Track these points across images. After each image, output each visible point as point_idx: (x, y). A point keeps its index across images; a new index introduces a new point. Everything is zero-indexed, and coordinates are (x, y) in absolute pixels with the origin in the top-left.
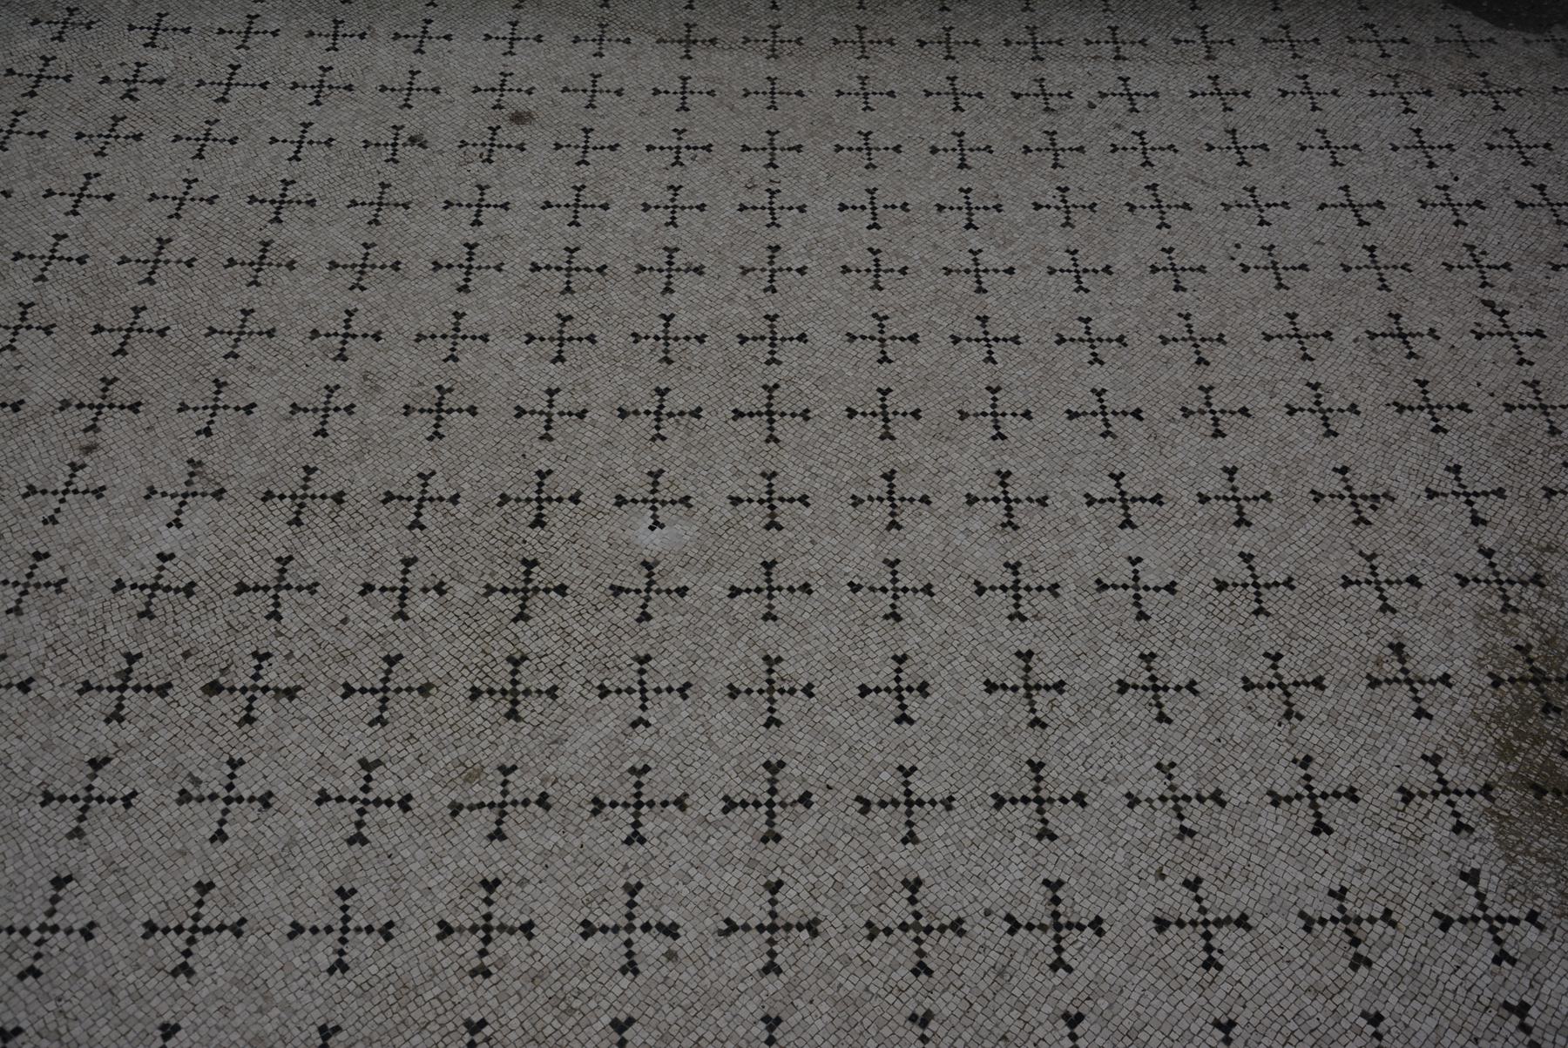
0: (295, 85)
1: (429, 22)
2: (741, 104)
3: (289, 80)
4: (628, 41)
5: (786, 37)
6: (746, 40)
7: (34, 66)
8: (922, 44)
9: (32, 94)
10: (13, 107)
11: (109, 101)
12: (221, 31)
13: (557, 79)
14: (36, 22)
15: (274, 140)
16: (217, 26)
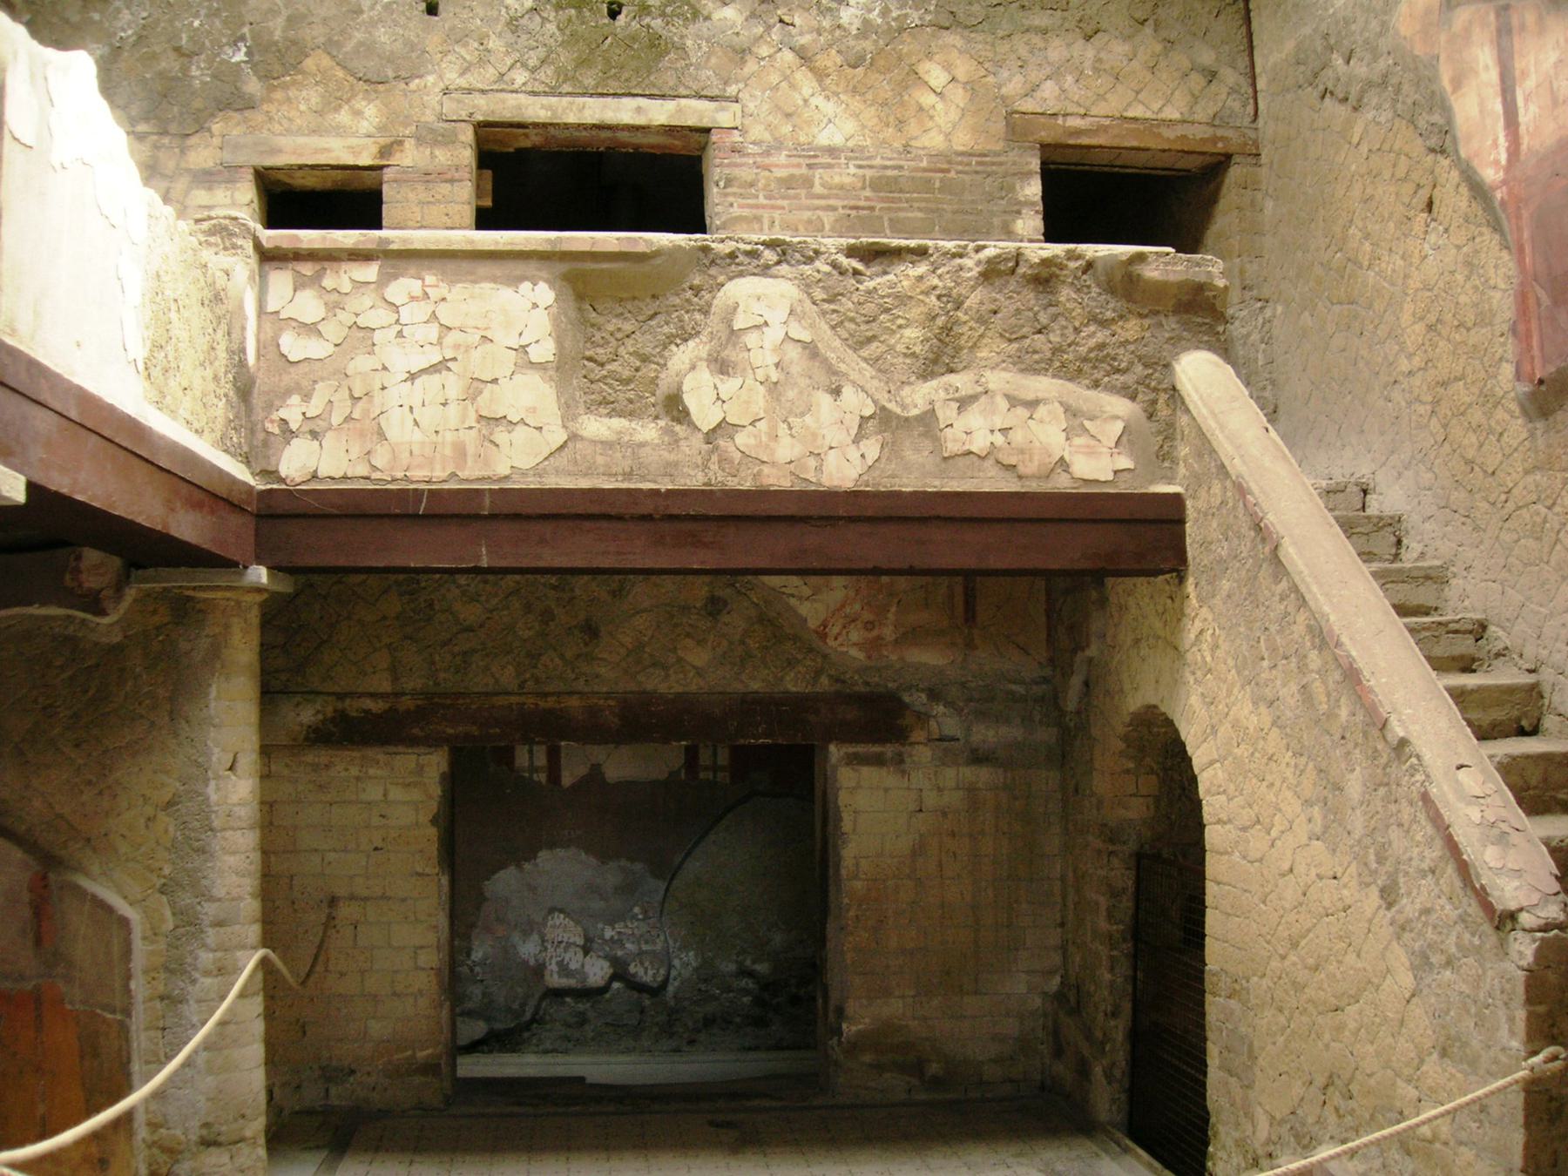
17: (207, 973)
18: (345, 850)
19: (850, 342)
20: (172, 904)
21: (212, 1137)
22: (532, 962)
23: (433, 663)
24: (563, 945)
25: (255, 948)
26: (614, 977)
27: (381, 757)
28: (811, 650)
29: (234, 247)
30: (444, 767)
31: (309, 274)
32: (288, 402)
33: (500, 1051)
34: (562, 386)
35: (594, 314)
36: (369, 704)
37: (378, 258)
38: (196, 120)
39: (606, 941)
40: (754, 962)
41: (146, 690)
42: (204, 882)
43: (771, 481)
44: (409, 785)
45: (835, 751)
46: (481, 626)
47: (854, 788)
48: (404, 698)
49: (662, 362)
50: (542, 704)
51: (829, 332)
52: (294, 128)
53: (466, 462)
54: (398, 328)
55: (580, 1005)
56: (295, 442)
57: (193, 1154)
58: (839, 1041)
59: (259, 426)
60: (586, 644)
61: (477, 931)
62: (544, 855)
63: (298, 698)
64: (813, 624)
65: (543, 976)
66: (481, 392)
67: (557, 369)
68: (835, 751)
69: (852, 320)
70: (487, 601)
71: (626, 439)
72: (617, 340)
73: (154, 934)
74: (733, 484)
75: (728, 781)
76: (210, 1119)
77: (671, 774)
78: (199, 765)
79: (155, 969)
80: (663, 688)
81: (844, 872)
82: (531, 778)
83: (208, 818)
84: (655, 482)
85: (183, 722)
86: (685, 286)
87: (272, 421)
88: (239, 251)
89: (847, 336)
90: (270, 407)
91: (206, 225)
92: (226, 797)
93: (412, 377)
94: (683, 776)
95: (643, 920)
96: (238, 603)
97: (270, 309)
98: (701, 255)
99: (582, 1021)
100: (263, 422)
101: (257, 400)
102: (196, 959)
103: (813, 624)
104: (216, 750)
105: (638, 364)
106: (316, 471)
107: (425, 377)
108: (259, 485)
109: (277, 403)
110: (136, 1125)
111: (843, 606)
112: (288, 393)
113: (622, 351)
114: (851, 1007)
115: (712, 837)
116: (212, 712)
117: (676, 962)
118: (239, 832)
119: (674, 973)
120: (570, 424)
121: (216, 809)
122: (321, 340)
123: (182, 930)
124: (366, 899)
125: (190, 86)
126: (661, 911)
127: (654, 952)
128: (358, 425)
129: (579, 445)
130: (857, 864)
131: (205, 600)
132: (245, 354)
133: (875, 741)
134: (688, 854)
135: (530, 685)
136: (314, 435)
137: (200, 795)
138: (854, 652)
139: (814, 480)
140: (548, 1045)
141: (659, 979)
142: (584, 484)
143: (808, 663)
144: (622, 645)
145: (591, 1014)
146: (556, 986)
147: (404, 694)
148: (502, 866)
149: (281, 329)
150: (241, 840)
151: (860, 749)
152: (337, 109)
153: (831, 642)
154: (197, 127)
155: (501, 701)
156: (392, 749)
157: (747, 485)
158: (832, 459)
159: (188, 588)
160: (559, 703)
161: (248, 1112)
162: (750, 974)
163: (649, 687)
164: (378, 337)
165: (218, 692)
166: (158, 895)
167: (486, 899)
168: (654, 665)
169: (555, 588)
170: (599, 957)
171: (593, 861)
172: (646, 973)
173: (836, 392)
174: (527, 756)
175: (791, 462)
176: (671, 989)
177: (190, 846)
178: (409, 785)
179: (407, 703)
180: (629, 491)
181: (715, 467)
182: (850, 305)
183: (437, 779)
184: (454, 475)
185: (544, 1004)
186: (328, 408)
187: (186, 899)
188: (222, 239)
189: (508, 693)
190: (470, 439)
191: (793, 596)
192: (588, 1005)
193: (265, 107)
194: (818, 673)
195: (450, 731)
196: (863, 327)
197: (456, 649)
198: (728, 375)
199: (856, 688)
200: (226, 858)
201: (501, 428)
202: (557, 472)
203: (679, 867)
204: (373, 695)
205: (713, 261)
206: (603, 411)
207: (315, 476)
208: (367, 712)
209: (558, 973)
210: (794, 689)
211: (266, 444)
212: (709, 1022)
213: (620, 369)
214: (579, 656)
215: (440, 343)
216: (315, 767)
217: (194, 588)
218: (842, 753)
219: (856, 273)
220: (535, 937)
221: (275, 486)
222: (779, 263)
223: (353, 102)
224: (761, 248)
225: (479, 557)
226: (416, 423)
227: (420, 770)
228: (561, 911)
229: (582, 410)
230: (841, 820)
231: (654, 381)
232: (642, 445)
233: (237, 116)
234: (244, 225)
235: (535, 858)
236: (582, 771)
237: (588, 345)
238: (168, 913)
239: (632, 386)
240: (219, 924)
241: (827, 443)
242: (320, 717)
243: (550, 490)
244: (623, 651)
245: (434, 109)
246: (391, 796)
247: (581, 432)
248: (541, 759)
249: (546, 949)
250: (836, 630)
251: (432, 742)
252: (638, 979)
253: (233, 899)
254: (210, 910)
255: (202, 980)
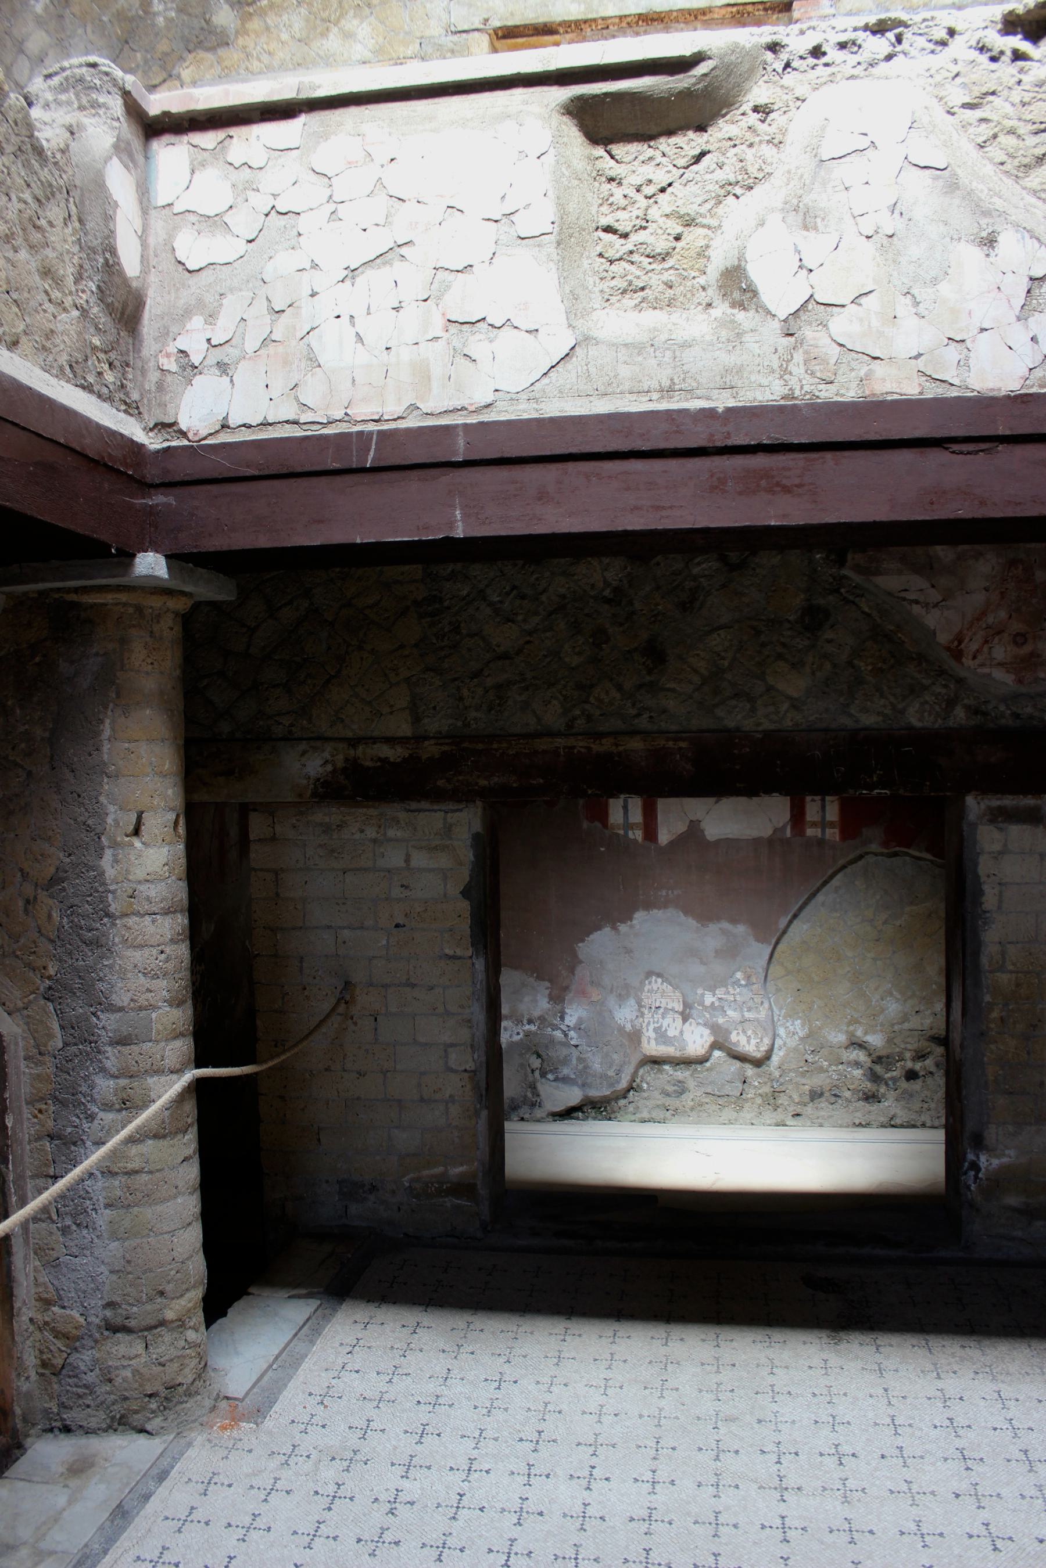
0: (503, 1510)
1: (593, 1467)
2: (830, 1539)
3: (499, 1506)
4: (737, 1487)
5: (853, 1488)
6: (824, 1489)
7: (331, 1489)
8: (957, 1496)
9: (330, 1509)
10: (317, 1518)
11: (378, 1516)
12: (452, 1469)
13: (689, 1514)
14: (333, 1459)
15: (490, 1551)
16: (449, 1465)
17: (107, 1107)
18: (362, 928)
19: (1008, 167)
20: (60, 1014)
21: (119, 1321)
22: (628, 1027)
23: (461, 699)
24: (662, 1010)
25: (179, 1071)
26: (715, 1046)
27: (402, 815)
28: (942, 672)
29: (95, 105)
30: (477, 826)
31: (210, 146)
32: (188, 327)
33: (595, 1119)
34: (566, 265)
35: (612, 163)
36: (386, 751)
37: (301, 111)
38: (163, 68)
39: (705, 1008)
40: (866, 1033)
41: (22, 729)
42: (100, 985)
43: (888, 387)
44: (436, 848)
45: (974, 805)
46: (519, 652)
47: (1000, 853)
48: (427, 743)
49: (713, 222)
50: (596, 748)
51: (975, 153)
52: (276, 63)
53: (430, 390)
54: (332, 207)
55: (679, 1073)
56: (198, 380)
57: (96, 1341)
58: (976, 1177)
59: (152, 364)
60: (650, 672)
61: (571, 995)
62: (639, 916)
63: (303, 746)
64: (943, 638)
65: (639, 1042)
66: (448, 287)
67: (559, 243)
68: (974, 805)
69: (1012, 132)
70: (525, 620)
71: (663, 337)
72: (646, 197)
73: (38, 1053)
74: (827, 394)
75: (838, 839)
76: (117, 1299)
77: (775, 830)
78: (89, 829)
79: (42, 1099)
80: (748, 725)
81: (984, 960)
82: (626, 833)
83: (103, 900)
84: (708, 398)
85: (66, 770)
86: (747, 107)
87: (168, 355)
88: (101, 112)
89: (1004, 158)
90: (165, 335)
91: (56, 80)
92: (128, 872)
93: (353, 272)
94: (788, 833)
95: (746, 985)
96: (139, 609)
97: (161, 202)
98: (769, 56)
99: (681, 1090)
100: (156, 356)
101: (148, 325)
102: (92, 1087)
103: (943, 638)
104: (112, 809)
105: (679, 229)
106: (226, 418)
107: (370, 273)
108: (153, 442)
109: (174, 329)
110: (17, 1305)
111: (984, 614)
112: (187, 313)
113: (654, 213)
114: (991, 1134)
115: (820, 897)
116: (106, 757)
117: (781, 1031)
118: (148, 918)
119: (778, 1042)
120: (579, 323)
121: (112, 888)
122: (229, 237)
123: (73, 1049)
124: (385, 986)
125: (154, 25)
126: (766, 977)
127: (757, 1020)
128: (281, 349)
129: (593, 351)
130: (1003, 954)
131: (93, 606)
132: (113, 251)
133: (1025, 792)
134: (795, 916)
135: (581, 723)
136: (223, 367)
137: (92, 868)
138: (998, 674)
139: (956, 381)
140: (645, 1115)
141: (764, 1048)
142: (602, 407)
143: (938, 689)
144: (696, 671)
145: (691, 1084)
146: (654, 1053)
147: (426, 738)
148: (598, 928)
149: (176, 228)
150: (151, 929)
151: (1008, 801)
152: (324, 34)
153: (967, 661)
154: (164, 75)
155: (543, 744)
156: (414, 805)
157: (851, 394)
158: (983, 347)
159: (69, 591)
160: (617, 745)
161: (169, 1288)
162: (861, 1046)
163: (731, 724)
164: (303, 223)
165: (113, 729)
166: (42, 1002)
167: (581, 962)
168: (736, 696)
169: (608, 601)
170: (698, 1024)
171: (692, 922)
172: (748, 1042)
173: (990, 242)
174: (621, 811)
175: (920, 355)
176: (775, 1059)
177: (78, 935)
178: (436, 848)
179: (431, 750)
180: (668, 413)
181: (798, 369)
182: (1009, 109)
183: (469, 842)
184: (414, 407)
185: (641, 1072)
186: (240, 330)
187: (78, 1008)
188: (77, 95)
189: (552, 734)
190: (435, 354)
191: (917, 602)
192: (687, 1073)
193: (241, 41)
194: (951, 703)
195: (483, 782)
196: (1032, 140)
197: (489, 682)
198: (816, 228)
199: (1003, 721)
200: (129, 953)
201: (478, 336)
202: (561, 394)
203: (784, 932)
204: (390, 740)
205: (787, 65)
206: (629, 301)
207: (225, 426)
208: (384, 760)
209: (656, 1039)
210: (918, 724)
211: (160, 386)
212: (815, 1095)
213: (651, 240)
214: (640, 686)
215: (387, 222)
216: (327, 829)
217: (76, 590)
218: (983, 806)
219: (1018, 56)
220: (632, 1002)
221: (174, 444)
222: (889, 58)
223: (343, 22)
224: (861, 36)
225: (451, 525)
226: (359, 338)
227: (448, 829)
228: (659, 975)
229: (597, 302)
230: (981, 893)
231: (702, 253)
232: (686, 345)
233: (209, 56)
234: (107, 74)
235: (631, 919)
236: (681, 828)
237: (605, 209)
238: (56, 1026)
239: (670, 262)
240: (123, 1041)
241: (977, 323)
242: (329, 768)
243: (552, 420)
244: (697, 679)
245: (440, 19)
246: (414, 863)
247: (594, 333)
248: (636, 816)
249: (642, 1015)
250: (974, 647)
251: (461, 796)
252: (740, 1049)
253: (141, 1008)
254: (108, 1022)
255: (101, 1115)
